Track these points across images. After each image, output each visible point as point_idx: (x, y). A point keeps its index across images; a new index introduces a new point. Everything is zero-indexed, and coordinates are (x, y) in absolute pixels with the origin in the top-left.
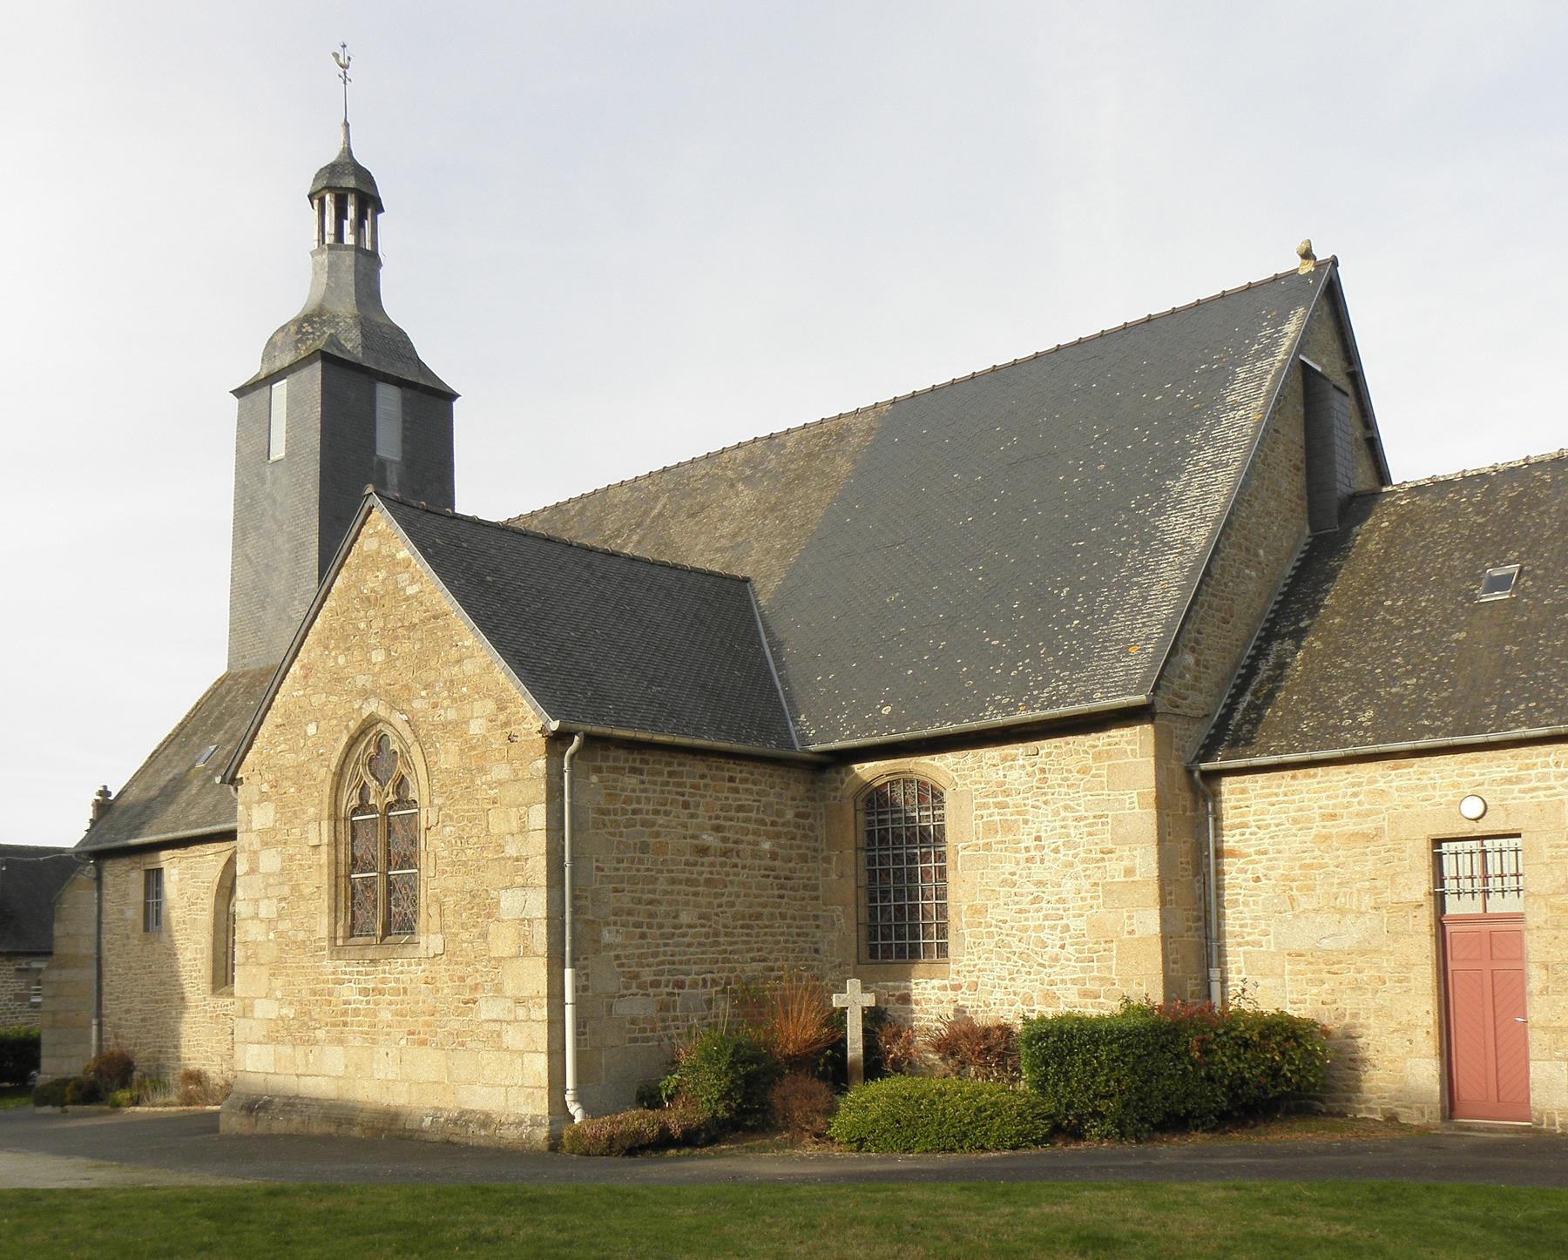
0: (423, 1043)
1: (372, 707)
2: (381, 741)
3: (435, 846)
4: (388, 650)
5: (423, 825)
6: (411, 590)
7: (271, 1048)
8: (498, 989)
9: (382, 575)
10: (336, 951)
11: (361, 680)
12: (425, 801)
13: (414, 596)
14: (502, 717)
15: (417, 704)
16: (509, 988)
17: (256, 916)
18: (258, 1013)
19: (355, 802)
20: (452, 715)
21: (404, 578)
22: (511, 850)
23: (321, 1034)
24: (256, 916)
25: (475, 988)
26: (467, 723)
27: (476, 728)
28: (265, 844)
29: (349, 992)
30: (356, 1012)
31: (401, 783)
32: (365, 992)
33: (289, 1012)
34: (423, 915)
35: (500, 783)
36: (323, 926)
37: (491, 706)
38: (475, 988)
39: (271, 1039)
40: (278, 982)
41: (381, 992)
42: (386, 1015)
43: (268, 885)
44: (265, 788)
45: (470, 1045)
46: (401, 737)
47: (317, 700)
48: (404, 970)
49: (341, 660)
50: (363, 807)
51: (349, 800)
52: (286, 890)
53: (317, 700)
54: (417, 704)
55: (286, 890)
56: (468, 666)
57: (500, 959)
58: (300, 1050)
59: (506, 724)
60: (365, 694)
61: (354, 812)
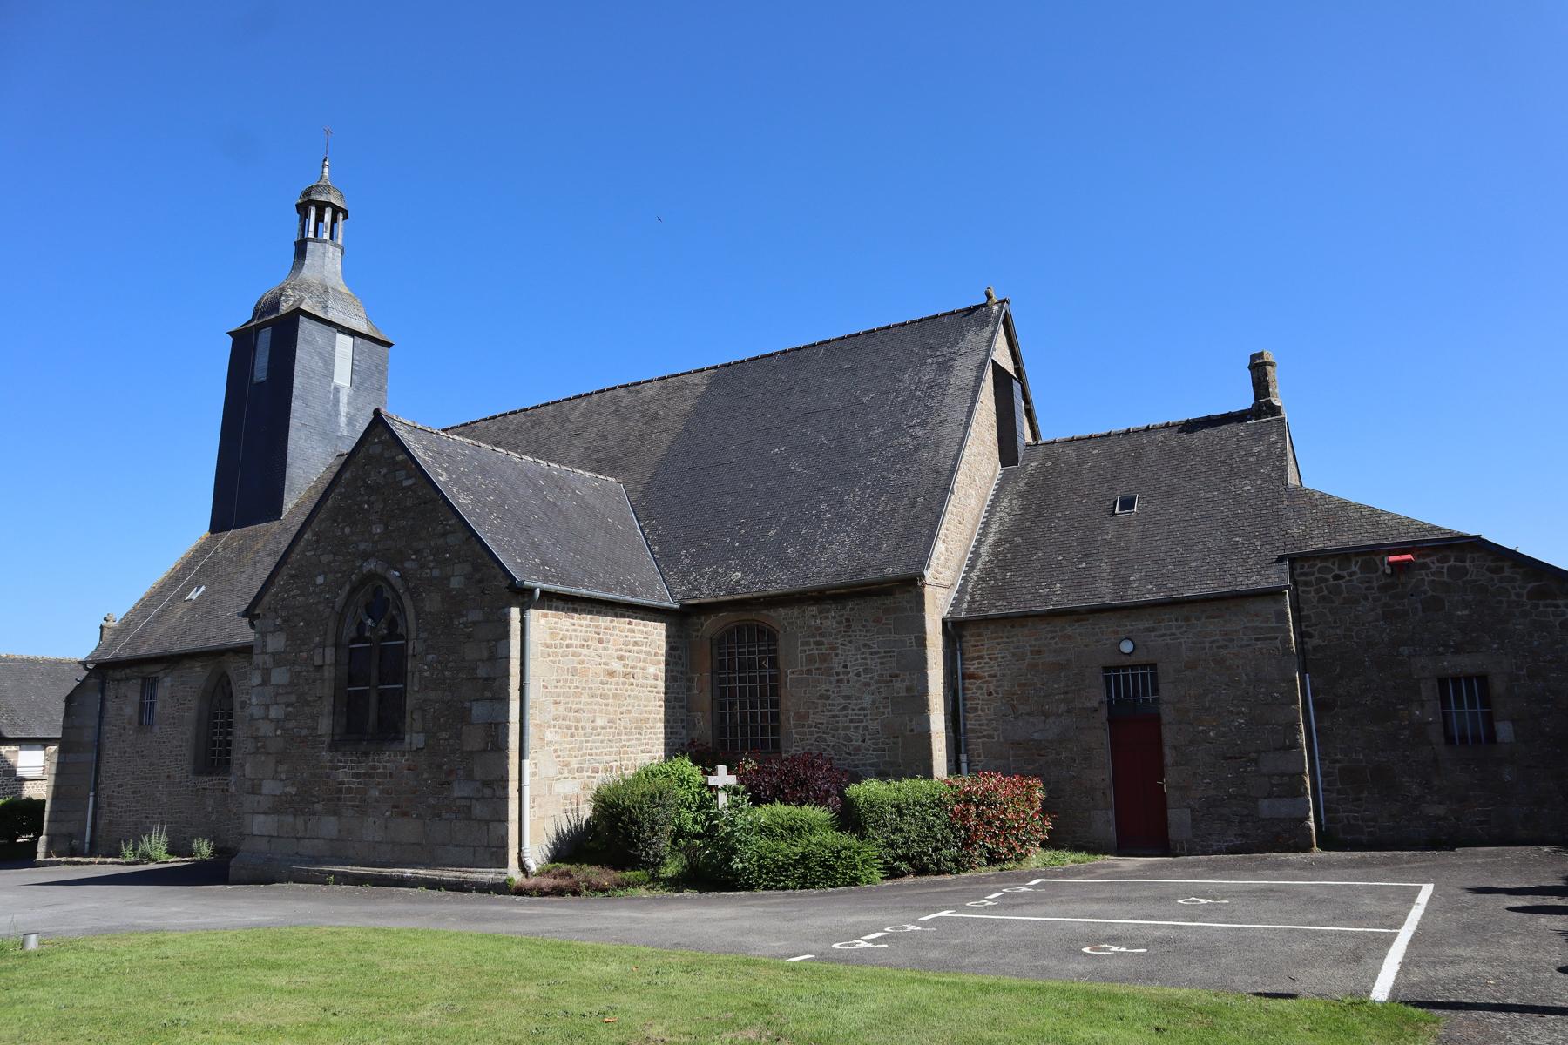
0: (405, 814)
1: (371, 565)
2: (377, 591)
3: (419, 669)
4: (386, 526)
5: (410, 652)
6: (406, 483)
7: (276, 818)
8: (470, 777)
9: (383, 471)
10: (334, 746)
11: (362, 546)
12: (413, 635)
13: (409, 487)
14: (477, 576)
15: (407, 565)
16: (478, 773)
17: (266, 718)
18: (265, 791)
19: (353, 634)
20: (436, 573)
21: (401, 474)
22: (481, 672)
23: (319, 807)
24: (266, 718)
25: (450, 773)
26: (448, 579)
27: (456, 583)
28: (278, 664)
29: (343, 775)
30: (349, 790)
31: (393, 624)
32: (357, 775)
33: (293, 791)
34: (408, 720)
35: (474, 623)
36: (325, 726)
37: (468, 568)
38: (450, 773)
39: (275, 810)
40: (284, 768)
41: (371, 776)
42: (375, 793)
43: (277, 694)
44: (279, 621)
45: (445, 815)
46: (393, 589)
47: (325, 559)
48: (391, 759)
49: (347, 530)
50: (360, 637)
51: (350, 631)
52: (293, 698)
53: (325, 559)
54: (407, 565)
55: (293, 698)
56: (451, 539)
57: (471, 752)
58: (300, 821)
59: (481, 581)
60: (366, 556)
61: (353, 641)
